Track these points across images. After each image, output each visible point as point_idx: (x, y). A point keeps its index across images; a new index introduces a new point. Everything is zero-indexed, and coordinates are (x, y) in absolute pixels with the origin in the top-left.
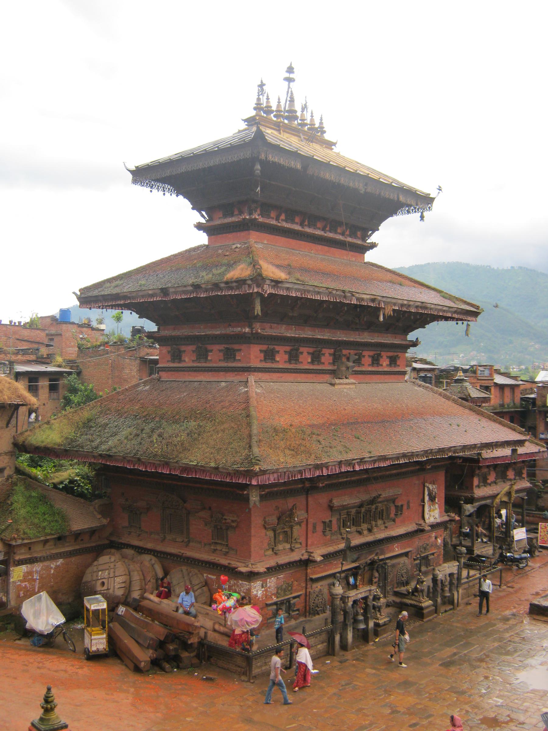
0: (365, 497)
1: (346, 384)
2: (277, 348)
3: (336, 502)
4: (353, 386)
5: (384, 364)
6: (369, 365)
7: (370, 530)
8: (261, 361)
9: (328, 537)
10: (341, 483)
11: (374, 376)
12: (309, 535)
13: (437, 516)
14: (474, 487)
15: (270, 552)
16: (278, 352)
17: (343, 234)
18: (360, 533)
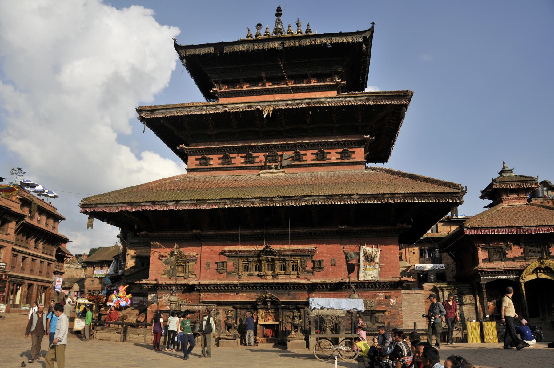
0: (261, 248)
1: (272, 173)
2: (211, 156)
3: (226, 249)
4: (284, 174)
5: (333, 158)
6: (313, 160)
7: (274, 276)
8: (196, 165)
9: (224, 274)
10: (233, 235)
11: (320, 168)
12: (203, 270)
13: (376, 275)
14: (480, 261)
15: (166, 276)
16: (212, 159)
17: (309, 82)
18: (259, 276)
